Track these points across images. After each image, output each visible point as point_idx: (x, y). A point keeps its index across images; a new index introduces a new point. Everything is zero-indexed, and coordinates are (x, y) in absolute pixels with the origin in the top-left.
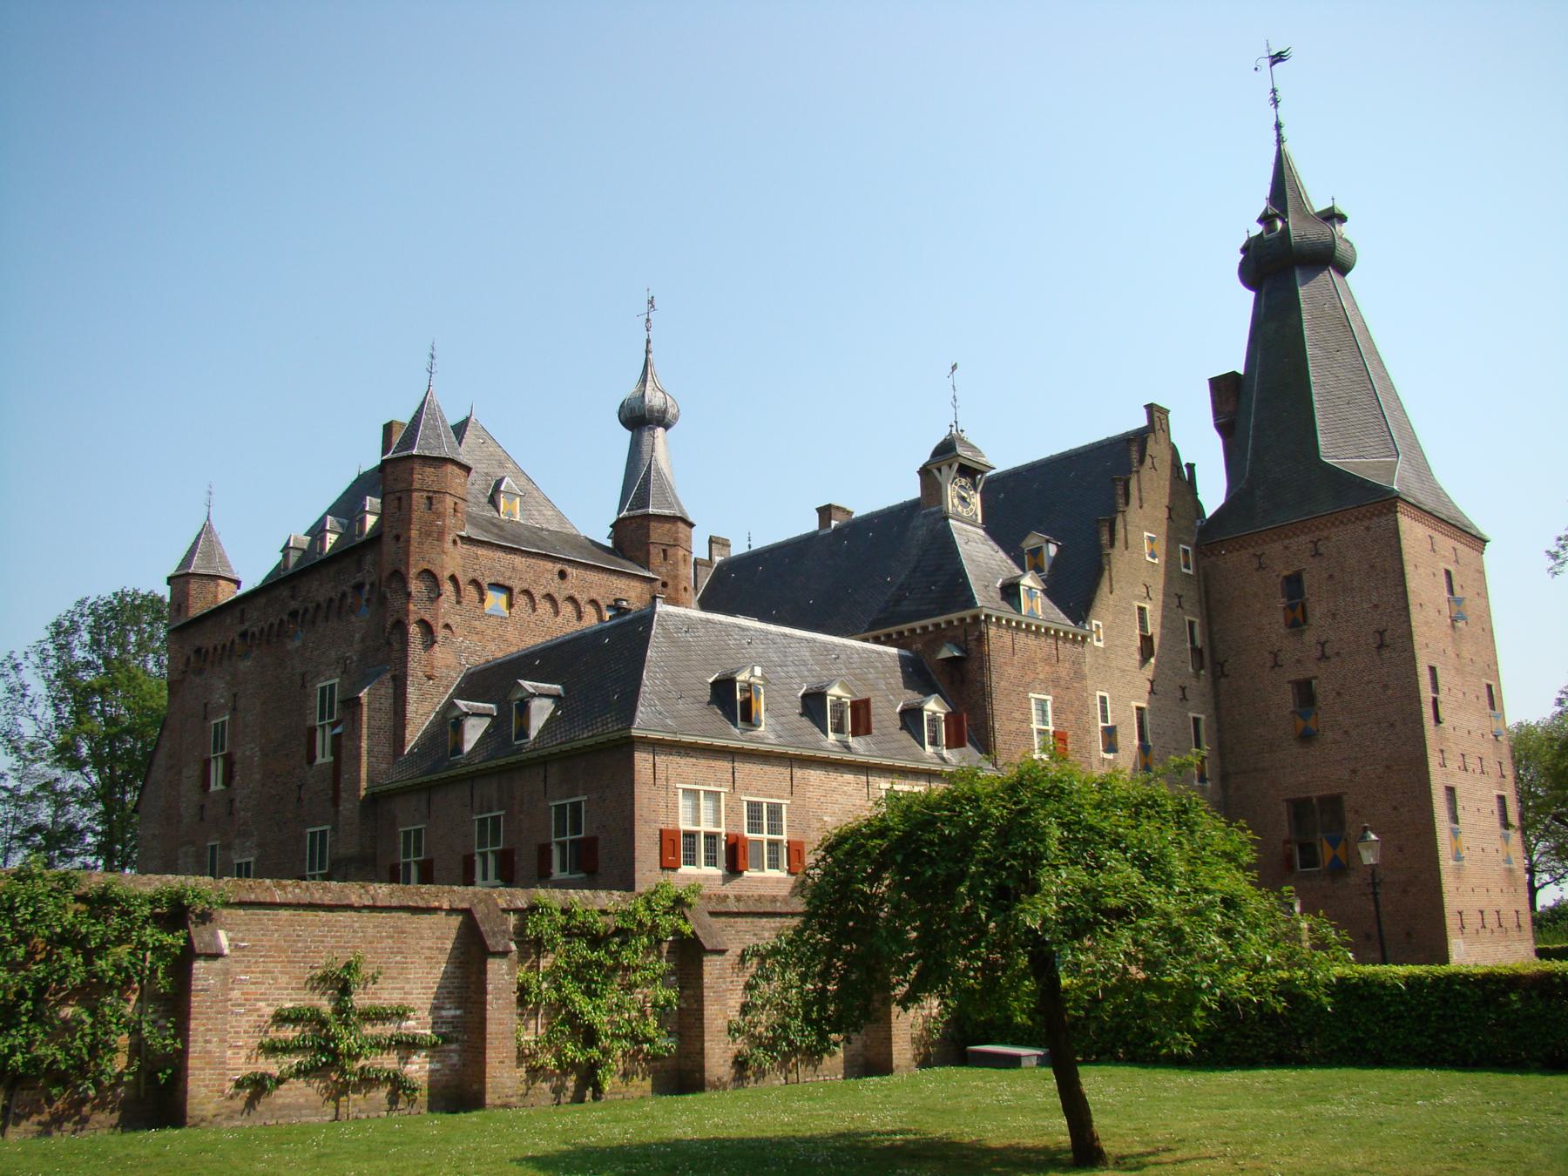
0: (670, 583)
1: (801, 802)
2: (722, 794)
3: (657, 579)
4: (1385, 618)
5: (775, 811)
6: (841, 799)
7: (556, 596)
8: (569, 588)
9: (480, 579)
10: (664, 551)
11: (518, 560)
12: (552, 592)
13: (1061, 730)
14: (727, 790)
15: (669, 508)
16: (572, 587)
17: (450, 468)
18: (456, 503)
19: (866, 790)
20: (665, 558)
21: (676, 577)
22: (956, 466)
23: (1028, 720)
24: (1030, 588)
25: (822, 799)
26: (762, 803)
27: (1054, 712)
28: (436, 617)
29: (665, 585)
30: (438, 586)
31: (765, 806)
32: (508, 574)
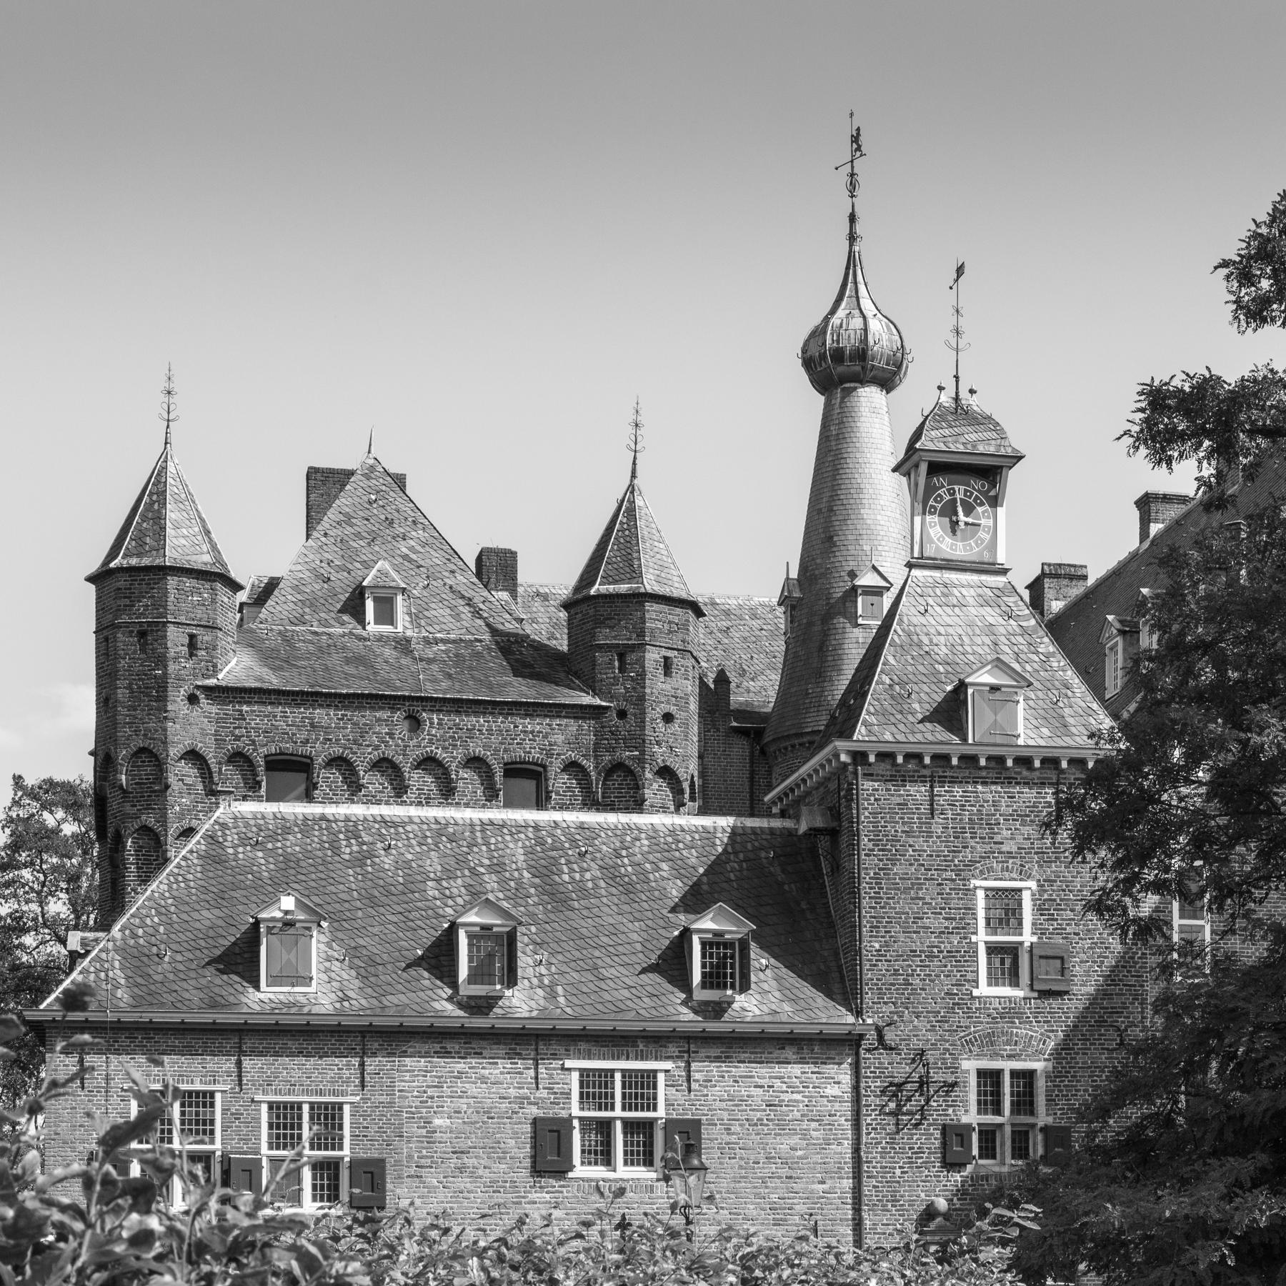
0: (631, 710)
1: (382, 1099)
2: (218, 1096)
3: (610, 707)
4: (241, 850)
5: (328, 1116)
6: (472, 1089)
7: (399, 759)
8: (423, 745)
9: (248, 750)
10: (621, 657)
11: (320, 714)
12: (390, 754)
13: (1059, 940)
14: (227, 1088)
15: (630, 580)
16: (431, 742)
17: (172, 582)
18: (192, 637)
19: (532, 1073)
20: (622, 670)
21: (642, 698)
22: (924, 468)
23: (966, 929)
24: (994, 688)
25: (430, 1092)
26: (300, 1105)
27: (1040, 909)
28: (163, 820)
29: (622, 714)
30: (161, 771)
31: (306, 1108)
32: (302, 736)
